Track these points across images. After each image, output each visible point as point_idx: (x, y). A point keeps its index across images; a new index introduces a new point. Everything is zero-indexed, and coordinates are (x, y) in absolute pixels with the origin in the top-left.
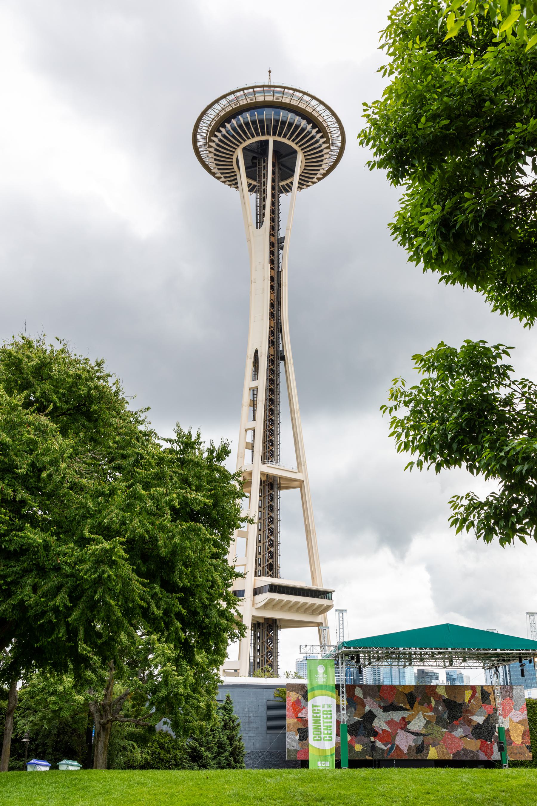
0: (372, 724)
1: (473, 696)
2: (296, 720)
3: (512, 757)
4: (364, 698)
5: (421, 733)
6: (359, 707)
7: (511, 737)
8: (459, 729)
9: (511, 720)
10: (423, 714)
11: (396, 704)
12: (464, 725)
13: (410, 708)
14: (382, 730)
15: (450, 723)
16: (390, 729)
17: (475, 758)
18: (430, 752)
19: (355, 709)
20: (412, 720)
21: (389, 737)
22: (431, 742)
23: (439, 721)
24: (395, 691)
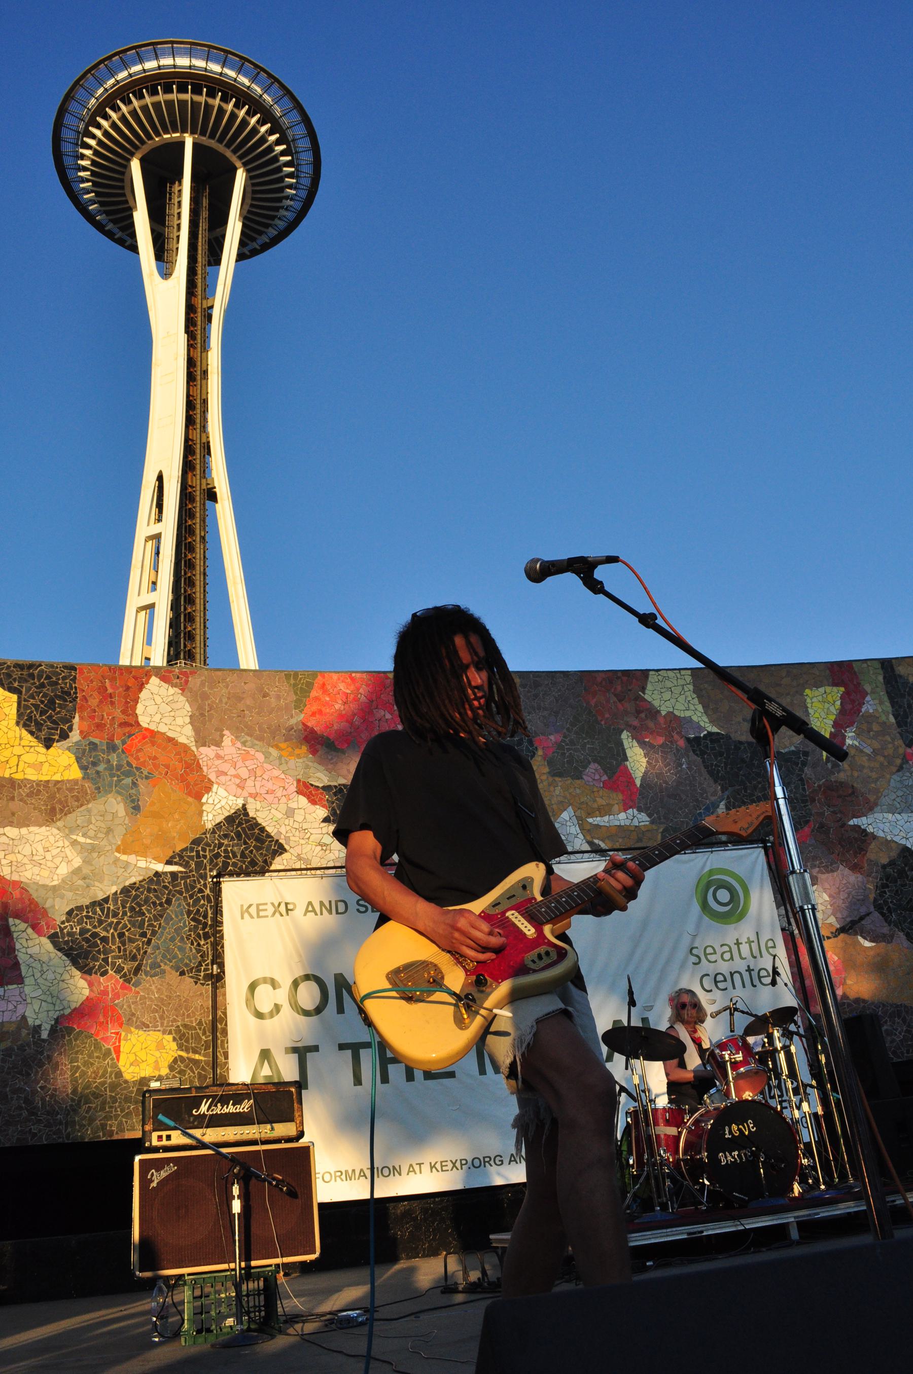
4: (202, 741)
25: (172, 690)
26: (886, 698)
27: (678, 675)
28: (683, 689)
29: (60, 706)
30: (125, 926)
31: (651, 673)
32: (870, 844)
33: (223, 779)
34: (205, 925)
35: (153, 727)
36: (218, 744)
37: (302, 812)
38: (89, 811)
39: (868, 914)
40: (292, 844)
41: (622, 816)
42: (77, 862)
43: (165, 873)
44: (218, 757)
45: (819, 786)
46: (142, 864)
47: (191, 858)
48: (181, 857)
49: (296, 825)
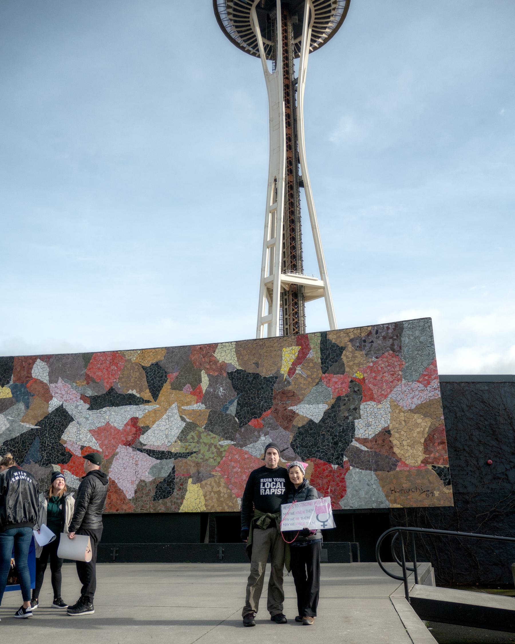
0: (59, 437)
1: (301, 359)
3: (395, 502)
4: (51, 382)
5: (169, 452)
6: (36, 401)
7: (396, 450)
8: (263, 438)
9: (395, 406)
10: (179, 407)
11: (120, 392)
12: (274, 428)
14: (82, 448)
15: (242, 424)
16: (101, 446)
18: (188, 495)
19: (27, 407)
20: (154, 422)
24: (121, 364)
25: (44, 363)
26: (319, 351)
27: (230, 345)
28: (231, 351)
29: (8, 372)
30: (20, 447)
31: (219, 344)
32: (295, 418)
33: (57, 395)
34: (45, 446)
35: (36, 377)
36: (56, 382)
37: (81, 406)
38: (13, 408)
39: (287, 448)
40: (76, 418)
41: (195, 405)
42: (8, 425)
43: (34, 429)
45: (279, 392)
46: (28, 426)
47: (43, 423)
48: (40, 423)
49: (78, 411)
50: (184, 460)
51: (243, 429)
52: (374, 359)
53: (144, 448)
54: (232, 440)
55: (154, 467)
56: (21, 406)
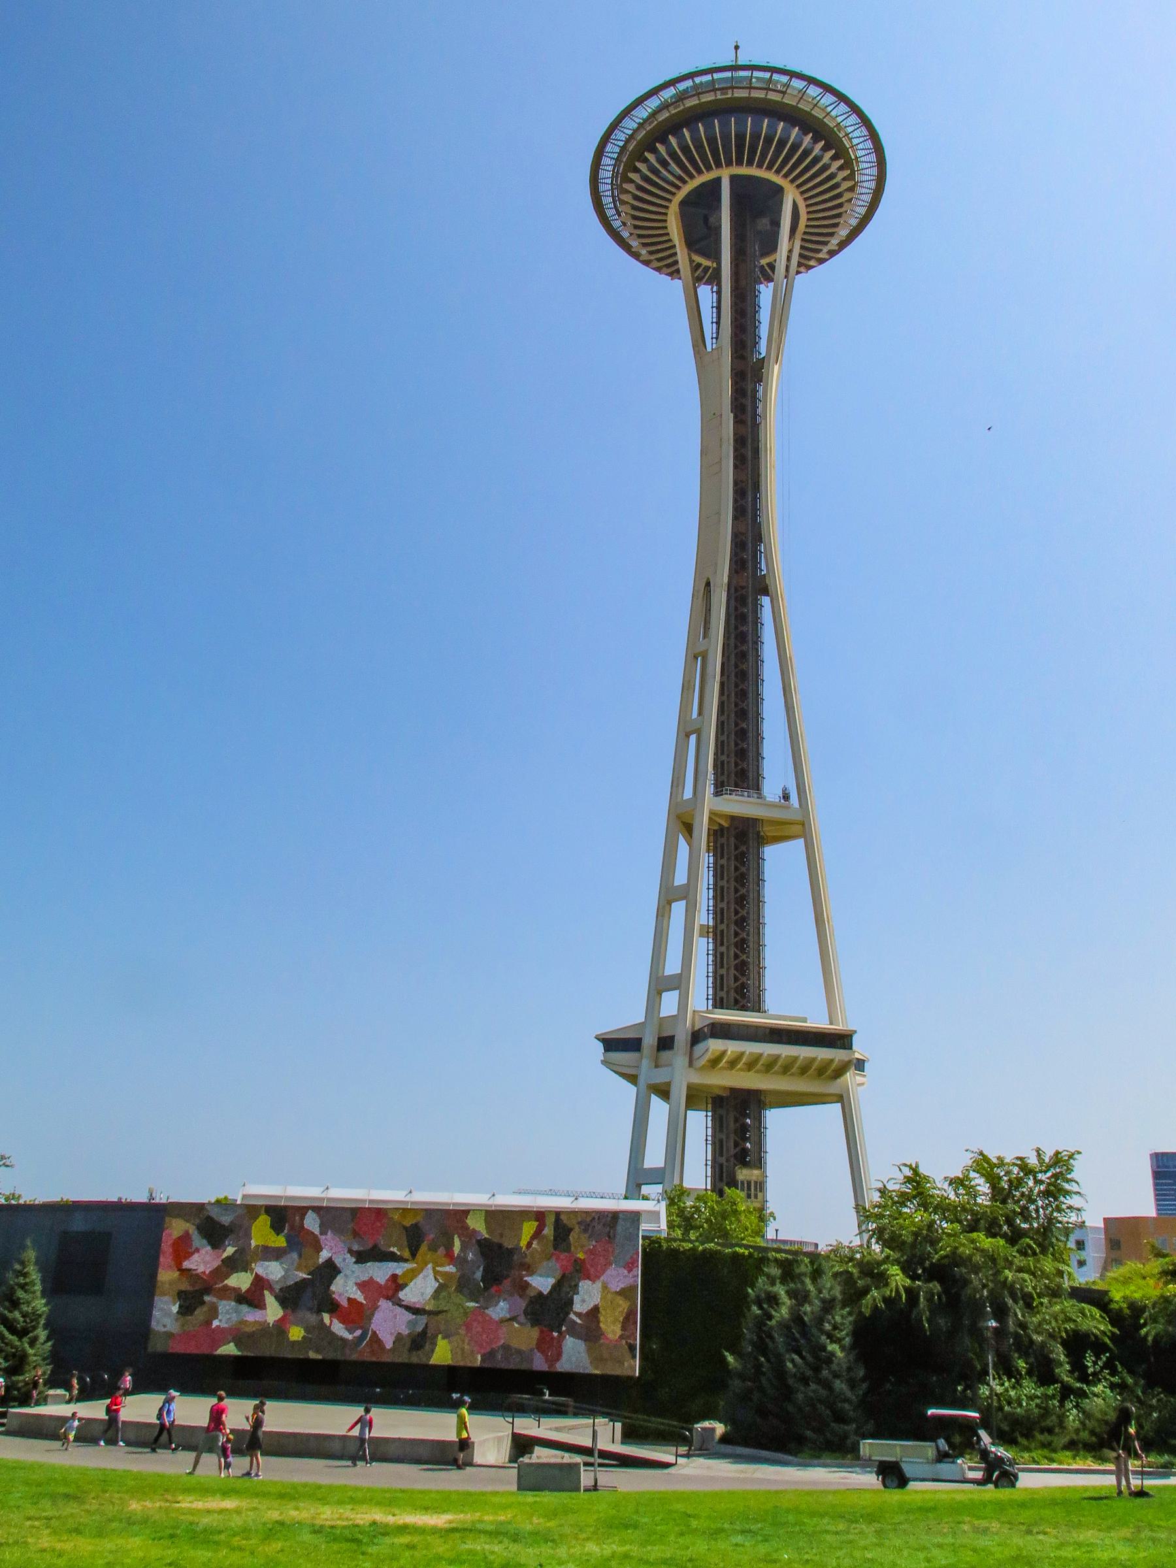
1: (537, 1234)
2: (177, 1274)
3: (597, 1368)
4: (321, 1234)
6: (308, 1251)
7: (602, 1325)
8: (502, 1304)
9: (605, 1287)
10: (434, 1269)
11: (383, 1249)
12: (512, 1295)
13: (410, 1258)
14: (349, 1299)
15: (486, 1288)
17: (524, 1366)
18: (437, 1349)
19: (300, 1256)
21: (355, 1314)
22: (442, 1328)
23: (464, 1285)
36: (326, 1234)
44: (326, 1239)
50: (436, 1318)
51: (486, 1294)
52: (594, 1243)
53: (403, 1303)
54: (477, 1302)
55: (410, 1321)
56: (295, 1255)
